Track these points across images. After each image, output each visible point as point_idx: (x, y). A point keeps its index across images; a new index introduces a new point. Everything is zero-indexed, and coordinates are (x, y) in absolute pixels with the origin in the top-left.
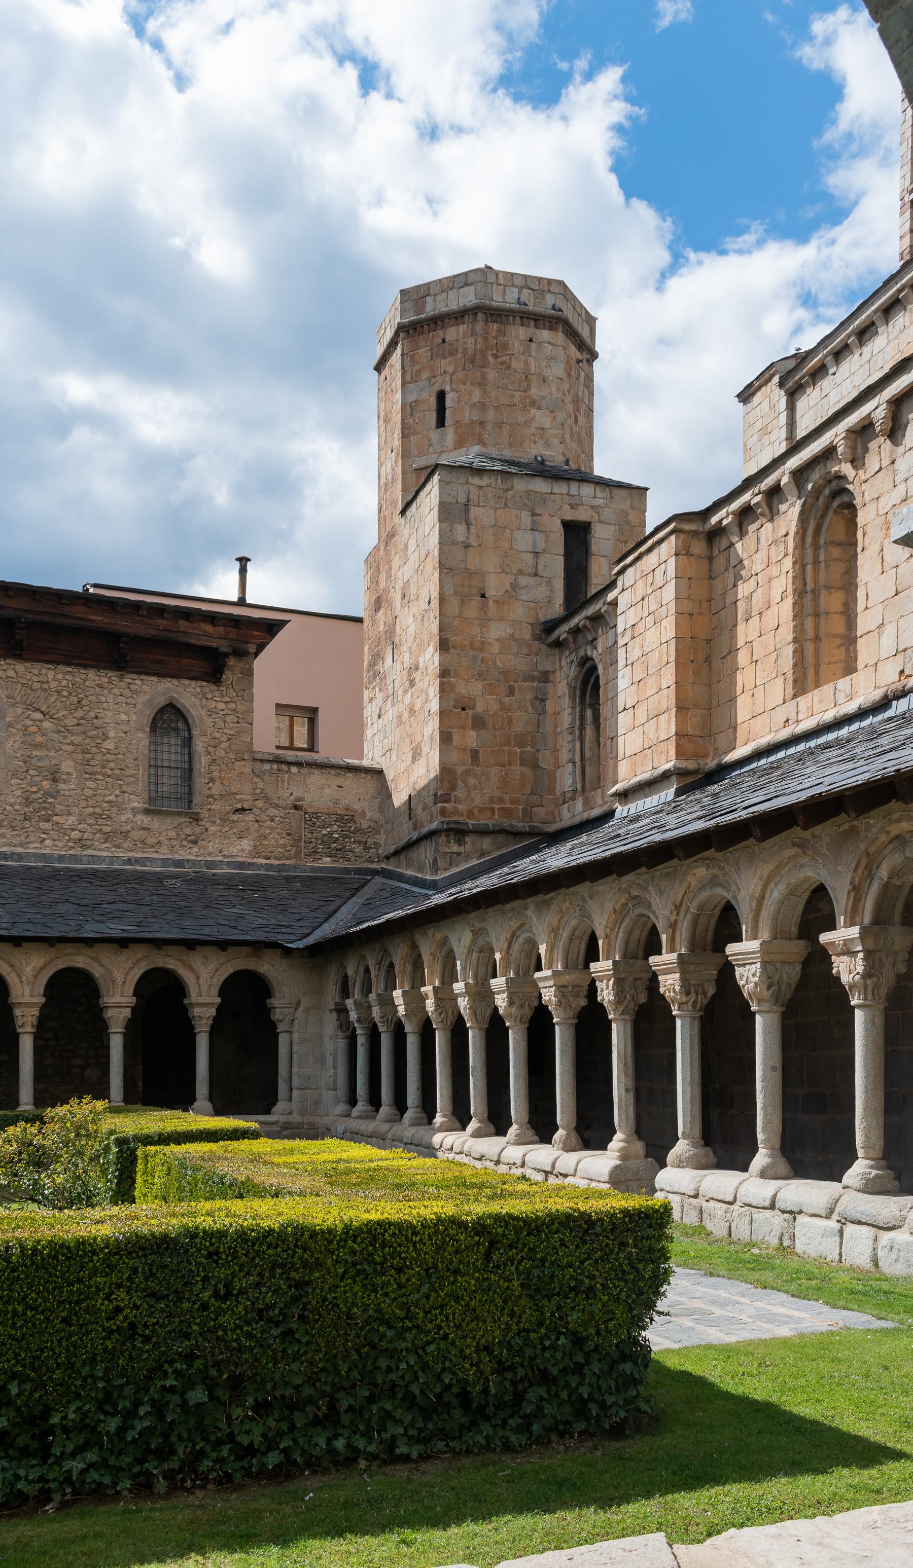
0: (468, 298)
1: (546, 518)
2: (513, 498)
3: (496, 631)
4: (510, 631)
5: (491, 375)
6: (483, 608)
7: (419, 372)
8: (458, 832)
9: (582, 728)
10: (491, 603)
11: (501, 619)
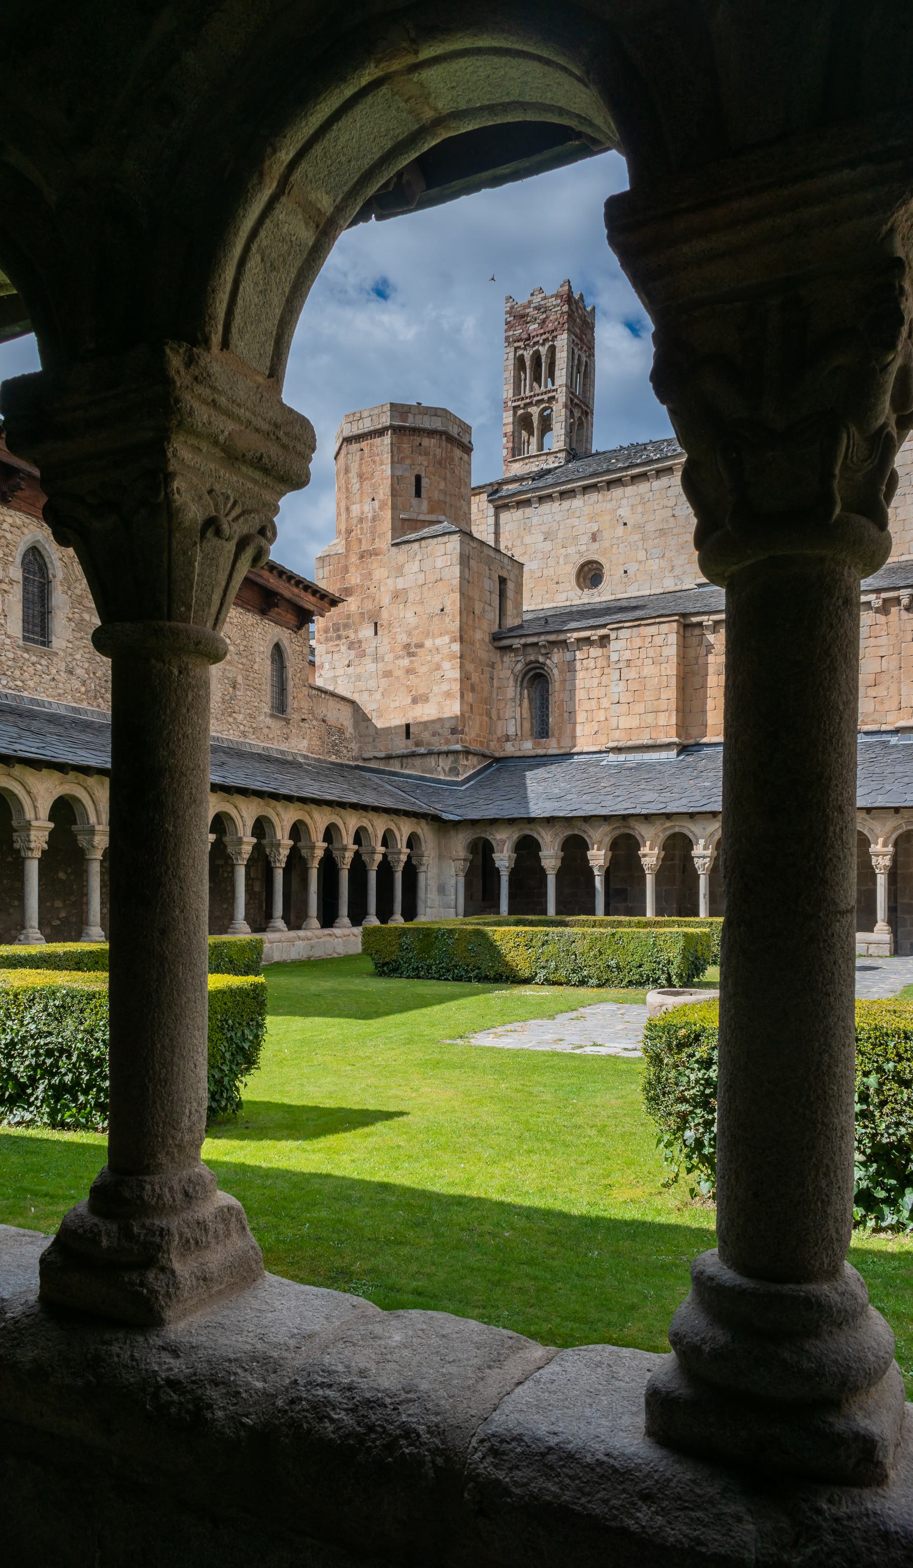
3: (478, 635)
5: (448, 475)
6: (474, 620)
7: (403, 458)
8: (467, 753)
9: (521, 700)
11: (480, 628)
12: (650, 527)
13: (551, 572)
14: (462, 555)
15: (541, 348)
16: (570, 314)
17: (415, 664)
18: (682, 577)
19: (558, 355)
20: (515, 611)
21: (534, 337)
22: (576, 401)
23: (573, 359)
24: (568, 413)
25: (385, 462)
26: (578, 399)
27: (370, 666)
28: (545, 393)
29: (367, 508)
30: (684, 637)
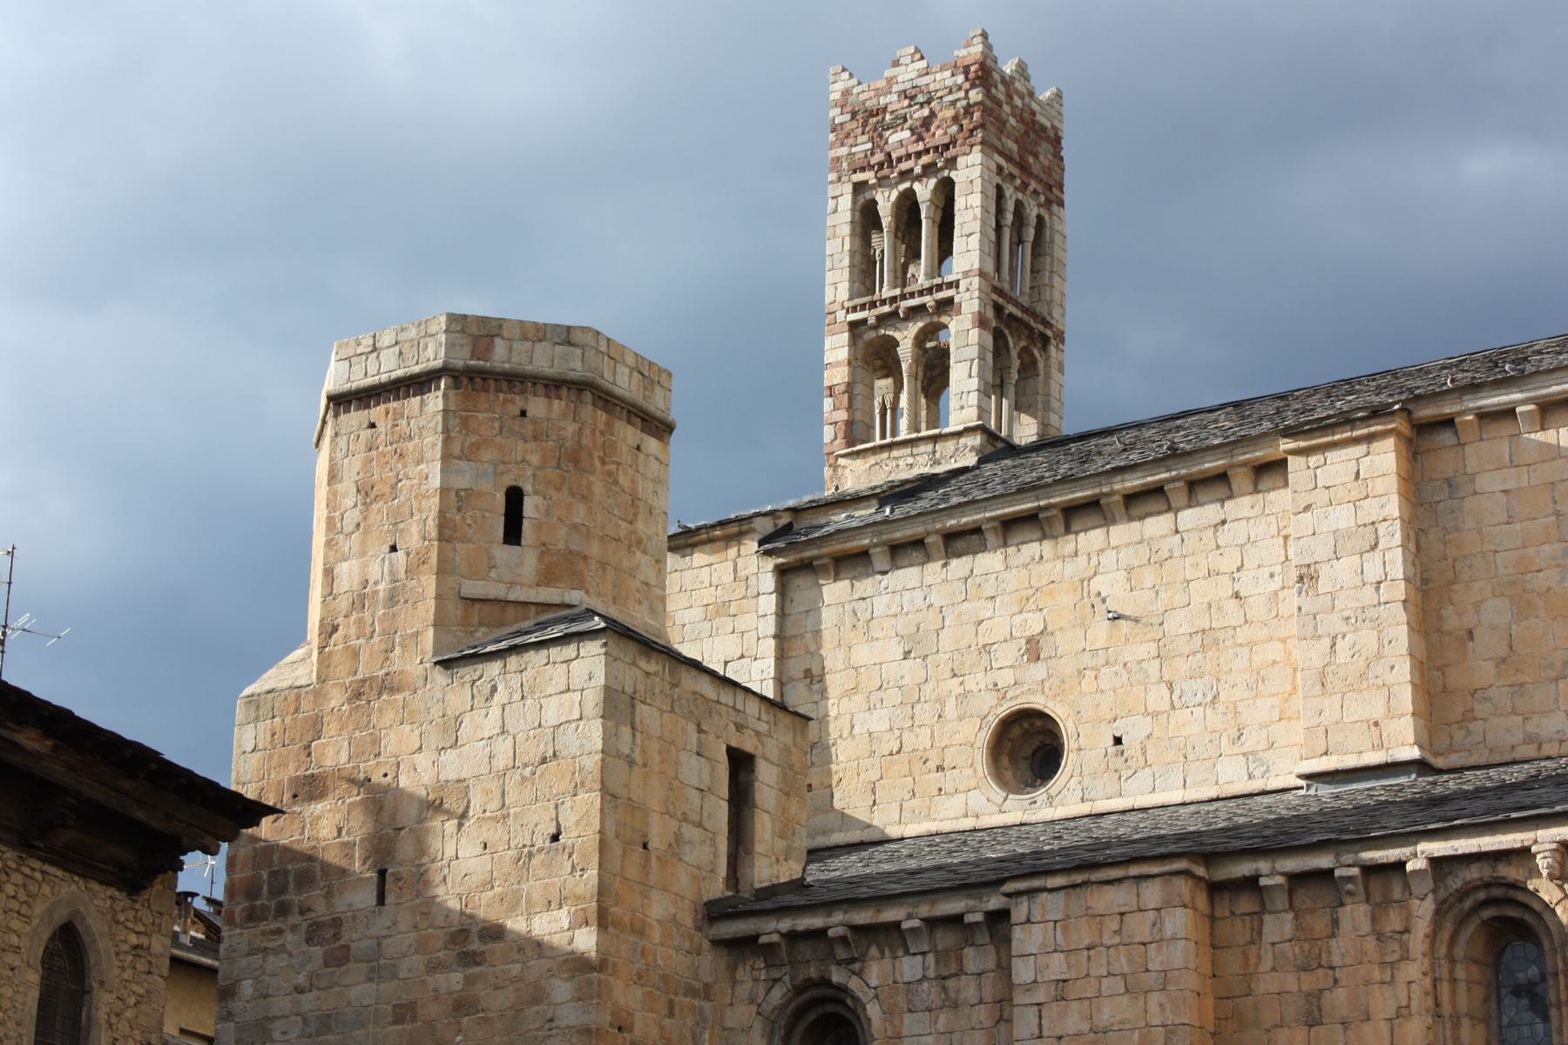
0: (575, 366)
1: (711, 738)
2: (680, 699)
3: (658, 908)
4: (672, 910)
5: (598, 489)
6: (645, 866)
7: (476, 447)
10: (654, 862)
11: (664, 889)
12: (1178, 624)
13: (919, 740)
14: (611, 695)
15: (917, 186)
16: (990, 109)
17: (479, 986)
18: (1268, 755)
19: (959, 203)
20: (781, 844)
21: (899, 160)
22: (1010, 309)
23: (1000, 211)
24: (989, 340)
25: (428, 455)
26: (1017, 304)
27: (359, 991)
28: (930, 291)
29: (374, 571)
30: (1212, 918)
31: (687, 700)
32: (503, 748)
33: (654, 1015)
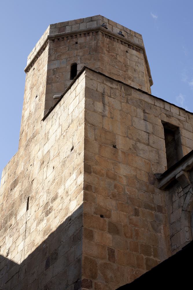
0: (94, 25)
5: (106, 58)
6: (115, 154)
10: (120, 153)
31: (136, 101)
32: (60, 130)
33: (125, 213)
